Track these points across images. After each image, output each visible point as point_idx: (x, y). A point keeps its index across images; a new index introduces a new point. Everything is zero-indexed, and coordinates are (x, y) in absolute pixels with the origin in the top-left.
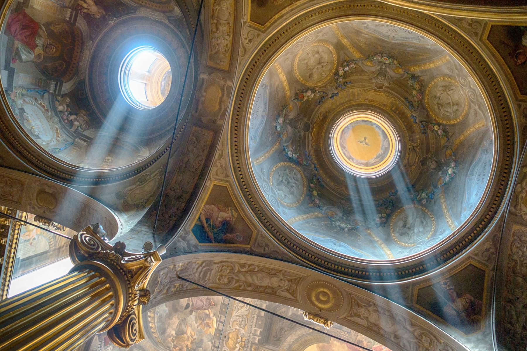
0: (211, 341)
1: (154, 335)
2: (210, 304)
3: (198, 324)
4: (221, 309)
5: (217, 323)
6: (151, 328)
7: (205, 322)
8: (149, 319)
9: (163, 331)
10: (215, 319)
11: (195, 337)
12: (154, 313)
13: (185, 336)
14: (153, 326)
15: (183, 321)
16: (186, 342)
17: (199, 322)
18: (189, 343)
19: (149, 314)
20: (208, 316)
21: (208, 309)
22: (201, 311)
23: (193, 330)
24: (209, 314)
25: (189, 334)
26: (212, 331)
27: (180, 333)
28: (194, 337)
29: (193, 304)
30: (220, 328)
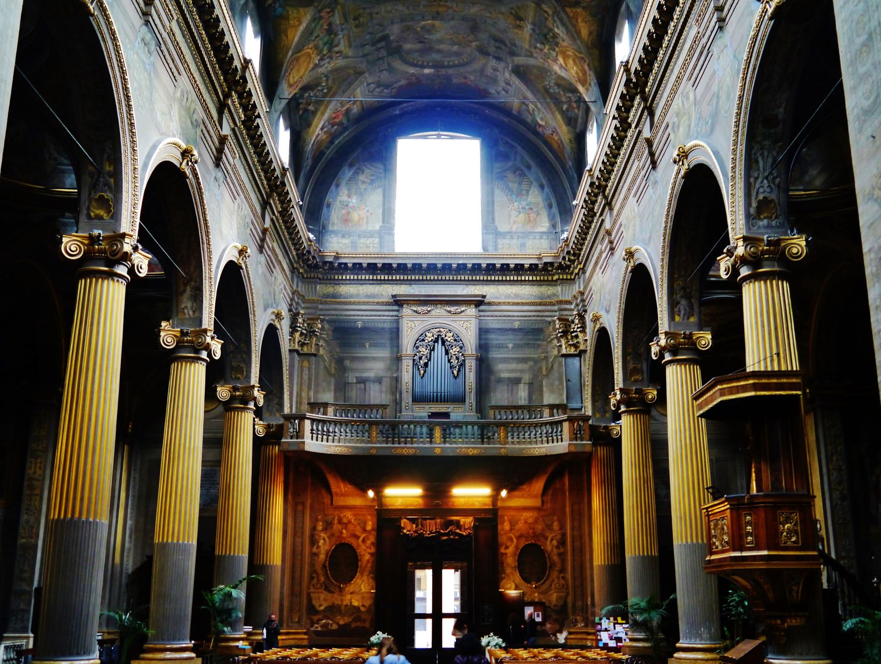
10: (423, 23)
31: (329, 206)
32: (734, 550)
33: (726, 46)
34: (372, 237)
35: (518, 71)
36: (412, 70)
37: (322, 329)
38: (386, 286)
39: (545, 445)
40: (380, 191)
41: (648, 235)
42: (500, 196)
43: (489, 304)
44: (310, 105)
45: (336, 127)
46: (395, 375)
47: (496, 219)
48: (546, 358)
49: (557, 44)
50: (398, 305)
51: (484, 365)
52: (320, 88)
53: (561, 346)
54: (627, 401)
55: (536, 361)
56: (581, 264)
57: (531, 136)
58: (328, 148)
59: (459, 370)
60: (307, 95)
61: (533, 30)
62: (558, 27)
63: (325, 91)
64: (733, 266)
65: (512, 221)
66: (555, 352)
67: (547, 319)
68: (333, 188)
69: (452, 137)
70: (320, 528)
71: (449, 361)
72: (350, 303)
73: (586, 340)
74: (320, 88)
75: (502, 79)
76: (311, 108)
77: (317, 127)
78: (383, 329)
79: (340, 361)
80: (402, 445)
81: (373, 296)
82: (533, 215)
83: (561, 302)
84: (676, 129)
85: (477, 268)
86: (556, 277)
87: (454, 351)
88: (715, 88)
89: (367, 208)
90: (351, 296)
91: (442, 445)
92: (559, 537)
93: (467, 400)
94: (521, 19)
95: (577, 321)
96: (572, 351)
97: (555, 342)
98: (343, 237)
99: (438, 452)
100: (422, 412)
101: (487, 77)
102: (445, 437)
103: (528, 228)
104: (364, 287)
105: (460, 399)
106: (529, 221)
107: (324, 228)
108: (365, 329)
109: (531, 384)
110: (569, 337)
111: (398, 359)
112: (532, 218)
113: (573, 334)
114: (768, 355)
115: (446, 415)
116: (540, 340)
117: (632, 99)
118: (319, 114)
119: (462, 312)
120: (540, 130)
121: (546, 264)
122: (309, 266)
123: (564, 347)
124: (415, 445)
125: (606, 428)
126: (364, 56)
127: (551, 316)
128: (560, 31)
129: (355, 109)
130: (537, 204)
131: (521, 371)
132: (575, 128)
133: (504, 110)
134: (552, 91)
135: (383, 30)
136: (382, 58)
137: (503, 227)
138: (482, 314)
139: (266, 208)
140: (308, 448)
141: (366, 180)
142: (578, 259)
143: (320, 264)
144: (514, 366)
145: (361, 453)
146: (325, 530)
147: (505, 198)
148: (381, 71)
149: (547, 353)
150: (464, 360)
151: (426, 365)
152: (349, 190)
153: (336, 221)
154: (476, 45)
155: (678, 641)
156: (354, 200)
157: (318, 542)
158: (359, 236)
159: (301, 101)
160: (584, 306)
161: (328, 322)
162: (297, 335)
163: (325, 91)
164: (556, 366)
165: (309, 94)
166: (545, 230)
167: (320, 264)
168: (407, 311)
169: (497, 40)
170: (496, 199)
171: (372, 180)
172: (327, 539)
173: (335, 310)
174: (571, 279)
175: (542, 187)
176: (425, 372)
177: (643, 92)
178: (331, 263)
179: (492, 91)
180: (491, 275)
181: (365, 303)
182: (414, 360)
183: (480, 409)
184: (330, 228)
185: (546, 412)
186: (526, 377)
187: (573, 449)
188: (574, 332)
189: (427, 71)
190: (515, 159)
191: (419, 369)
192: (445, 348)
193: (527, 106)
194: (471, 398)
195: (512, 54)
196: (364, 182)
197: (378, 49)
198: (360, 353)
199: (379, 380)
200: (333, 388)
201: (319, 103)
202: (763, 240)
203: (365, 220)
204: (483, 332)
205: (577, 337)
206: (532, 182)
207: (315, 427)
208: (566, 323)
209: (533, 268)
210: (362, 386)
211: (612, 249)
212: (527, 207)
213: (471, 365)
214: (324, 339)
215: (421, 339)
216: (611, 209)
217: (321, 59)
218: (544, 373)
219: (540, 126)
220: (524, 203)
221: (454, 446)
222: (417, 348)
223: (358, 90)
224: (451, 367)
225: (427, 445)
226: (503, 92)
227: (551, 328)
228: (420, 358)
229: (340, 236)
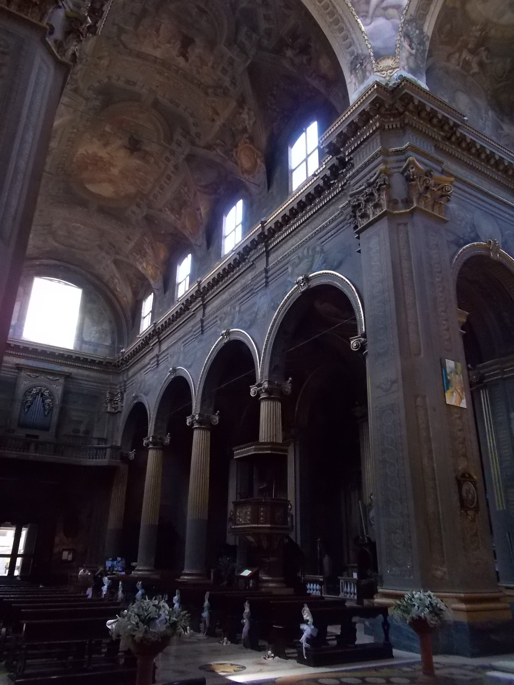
32: (254, 524)
33: (266, 294)
35: (116, 262)
36: (56, 244)
38: (12, 358)
39: (94, 460)
41: (190, 363)
49: (145, 257)
50: (18, 370)
51: (63, 411)
53: (107, 407)
54: (154, 443)
57: (111, 295)
59: (48, 413)
61: (134, 246)
62: (149, 249)
64: (258, 392)
69: (66, 284)
71: (44, 406)
82: (103, 336)
83: (111, 384)
84: (222, 320)
86: (111, 370)
88: (255, 309)
94: (130, 239)
96: (113, 410)
100: (21, 433)
102: (36, 449)
105: (47, 429)
110: (113, 403)
114: (272, 435)
115: (36, 437)
117: (196, 298)
120: (116, 293)
121: (108, 362)
125: (127, 454)
128: (149, 251)
133: (99, 278)
151: (29, 407)
155: (183, 569)
166: (108, 344)
168: (23, 374)
169: (111, 244)
175: (110, 322)
177: (203, 297)
180: (76, 363)
182: (22, 403)
183: (57, 435)
185: (96, 442)
188: (116, 401)
191: (24, 408)
192: (42, 399)
193: (114, 280)
194: (53, 430)
195: (117, 253)
202: (275, 383)
204: (66, 393)
205: (117, 403)
208: (113, 395)
209: (100, 363)
211: (158, 364)
213: (56, 411)
215: (29, 391)
219: (117, 291)
220: (100, 328)
222: (26, 396)
224: (44, 410)
228: (27, 402)
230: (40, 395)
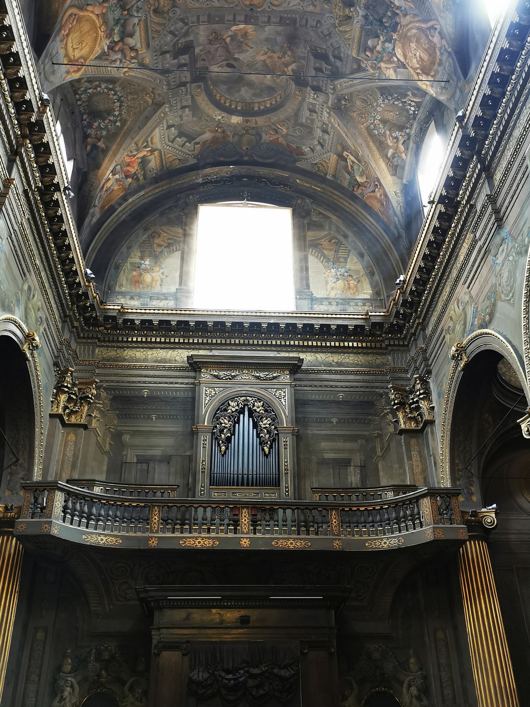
0: (263, 27)
1: (278, 100)
2: (216, 39)
3: (248, 48)
4: (218, 23)
5: (238, 25)
6: (271, 104)
7: (242, 40)
8: (262, 107)
9: (271, 90)
10: (234, 28)
11: (265, 48)
12: (253, 103)
13: (268, 61)
14: (269, 102)
15: (250, 65)
16: (275, 60)
17: (245, 47)
18: (275, 56)
19: (256, 109)
20: (233, 38)
21: (225, 40)
22: (230, 47)
23: (258, 53)
24: (230, 36)
25: (263, 58)
26: (250, 28)
27: (268, 70)
28: (267, 50)
29: (224, 60)
30: (243, 18)
31: (117, 267)
34: (166, 299)
37: (98, 396)
40: (178, 254)
42: (313, 262)
43: (307, 372)
44: (100, 140)
45: (130, 180)
46: (188, 453)
47: (311, 285)
48: (380, 436)
49: (394, 28)
50: (195, 371)
52: (111, 118)
53: (397, 422)
55: (368, 439)
56: (419, 318)
58: (120, 205)
59: (271, 447)
60: (96, 124)
63: (118, 124)
65: (329, 287)
66: (391, 429)
67: (377, 390)
68: (124, 249)
70: (68, 668)
71: (258, 435)
72: (135, 368)
73: (433, 408)
74: (111, 118)
75: (320, 124)
76: (101, 144)
77: (107, 169)
78: (175, 398)
79: (117, 436)
80: (195, 534)
81: (164, 361)
82: (352, 283)
85: (291, 329)
87: (265, 423)
89: (162, 271)
90: (138, 360)
91: (252, 535)
92: (419, 681)
93: (283, 484)
95: (418, 387)
97: (390, 417)
98: (132, 298)
99: (245, 543)
101: (302, 125)
103: (349, 296)
104: (154, 351)
106: (349, 288)
107: (109, 288)
108: (152, 398)
109: (363, 467)
110: (408, 410)
111: (193, 434)
112: (352, 285)
113: (413, 406)
116: (371, 414)
118: (110, 153)
119: (274, 378)
122: (86, 320)
123: (402, 421)
124: (213, 535)
126: (165, 72)
127: (382, 388)
129: (154, 163)
130: (358, 272)
131: (351, 451)
132: (401, 178)
134: (376, 132)
135: (187, 34)
136: (184, 84)
137: (318, 292)
138: (298, 383)
139: (15, 161)
140: (55, 531)
141: (162, 243)
142: (416, 311)
143: (101, 319)
144: (340, 444)
145: (135, 546)
146: (74, 670)
147: (321, 265)
148: (183, 108)
149: (381, 430)
150: (277, 435)
152: (142, 252)
153: (124, 282)
154: (293, 71)
156: (147, 262)
157: (63, 691)
158: (151, 298)
159: (89, 131)
160: (427, 366)
161: (106, 389)
162: (63, 398)
163: (118, 124)
164: (393, 445)
165: (99, 125)
167: (101, 319)
168: (205, 376)
170: (310, 265)
171: (169, 244)
172: (76, 686)
173: (116, 375)
174: (404, 345)
175: (361, 255)
176: (227, 448)
178: (114, 318)
179: (306, 149)
181: (153, 368)
182: (213, 433)
184: (117, 289)
186: (357, 459)
187: (441, 536)
188: (414, 403)
189: (235, 119)
190: (330, 229)
191: (219, 445)
192: (253, 420)
193: (345, 160)
196: (160, 245)
197: (181, 66)
198: (145, 426)
199: (167, 460)
200: (105, 468)
201: (111, 137)
203: (159, 282)
205: (418, 408)
206: (350, 251)
207: (70, 505)
210: (145, 466)
212: (346, 274)
214: (99, 409)
216: (490, 178)
217: (111, 48)
218: (379, 454)
219: (359, 185)
220: (343, 270)
221: (267, 536)
222: (218, 419)
223: (157, 131)
224: (261, 444)
225: (230, 535)
226: (319, 147)
227: (383, 401)
228: (222, 431)
229: (128, 297)
230: (246, 413)
